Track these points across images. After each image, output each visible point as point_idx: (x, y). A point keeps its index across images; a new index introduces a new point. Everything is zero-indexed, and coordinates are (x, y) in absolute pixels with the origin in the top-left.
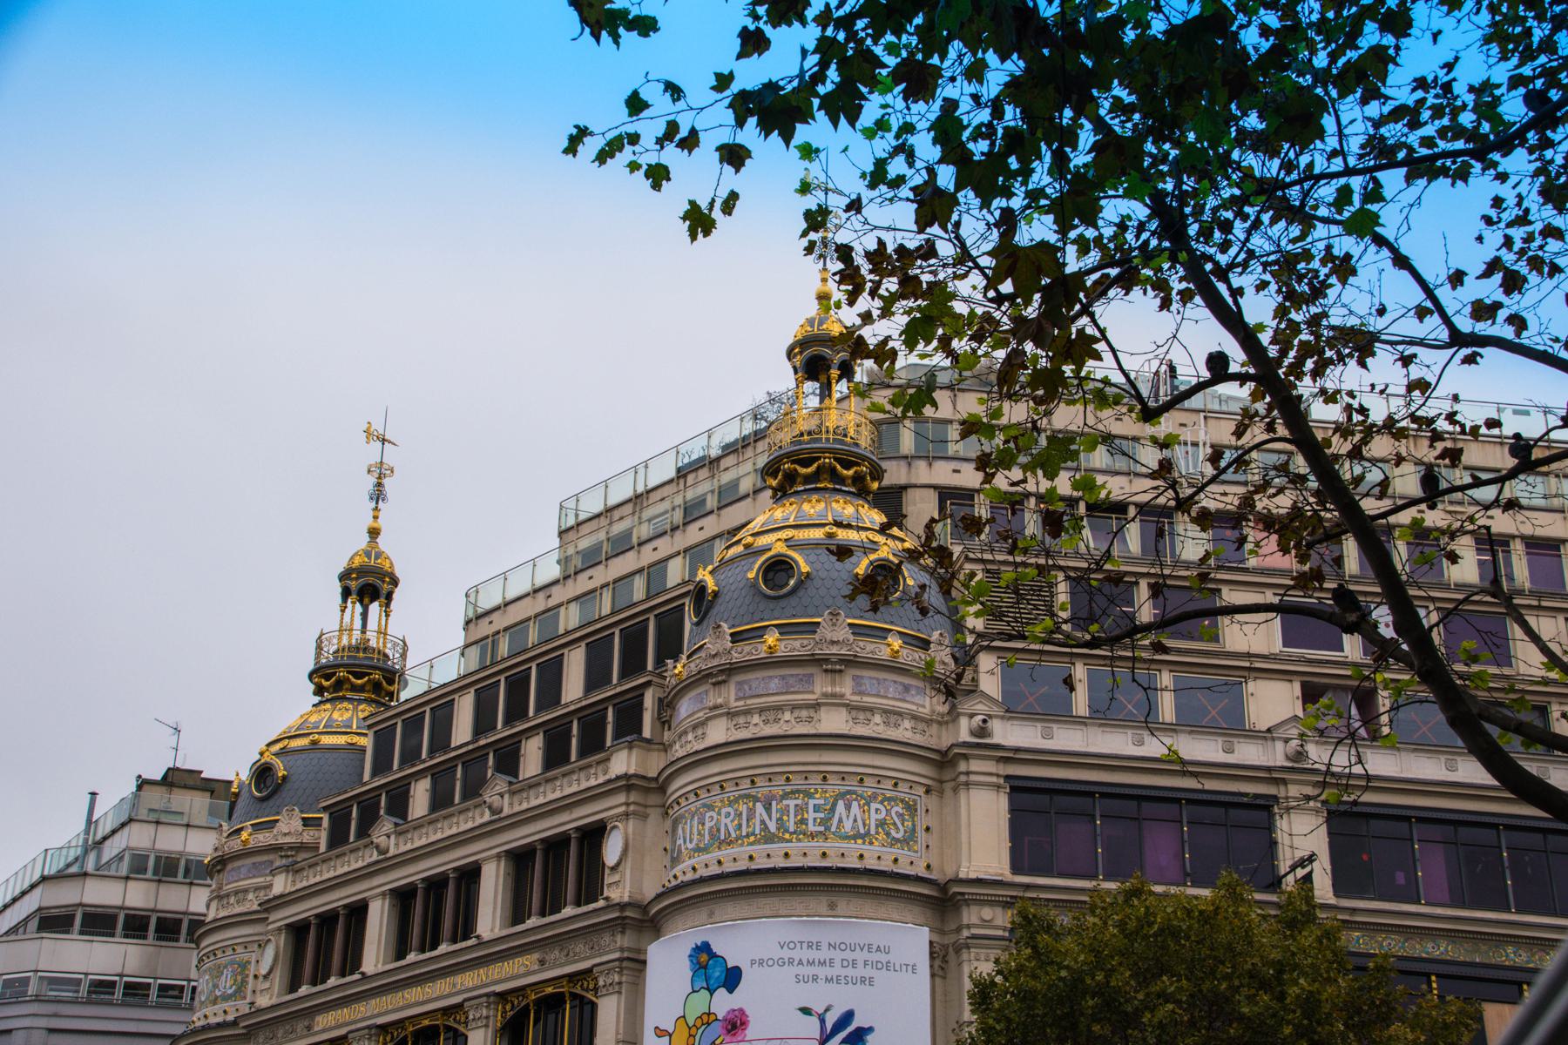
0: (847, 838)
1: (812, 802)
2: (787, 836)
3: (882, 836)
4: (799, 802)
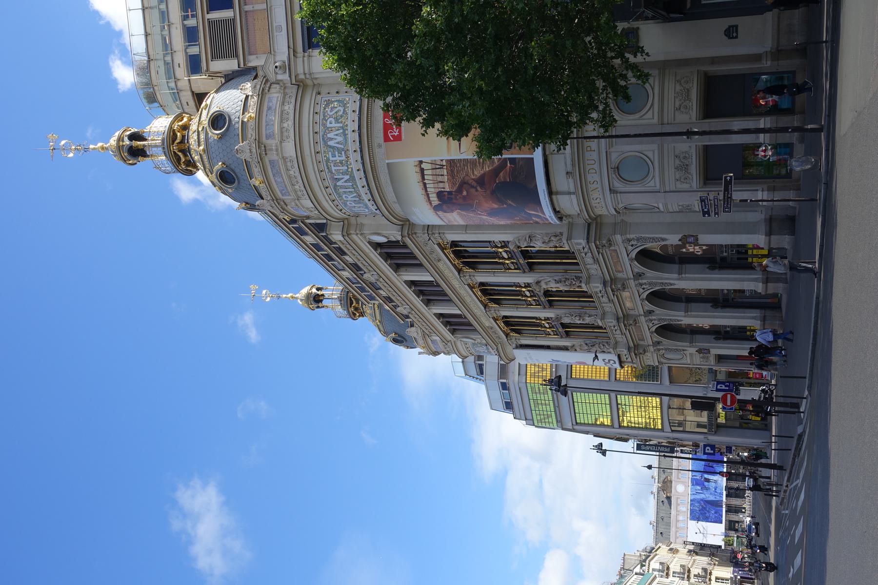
0: (346, 139)
1: (331, 158)
2: (350, 170)
3: (343, 120)
4: (332, 165)
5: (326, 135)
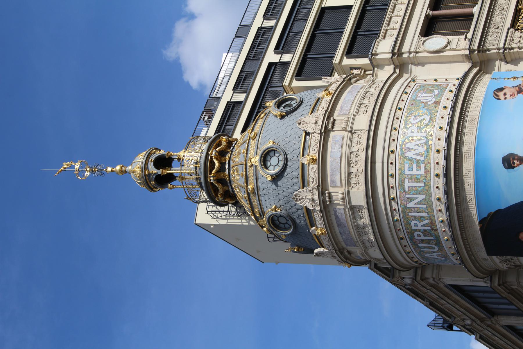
1: (407, 173)
3: (428, 129)
4: (406, 180)
5: (405, 145)
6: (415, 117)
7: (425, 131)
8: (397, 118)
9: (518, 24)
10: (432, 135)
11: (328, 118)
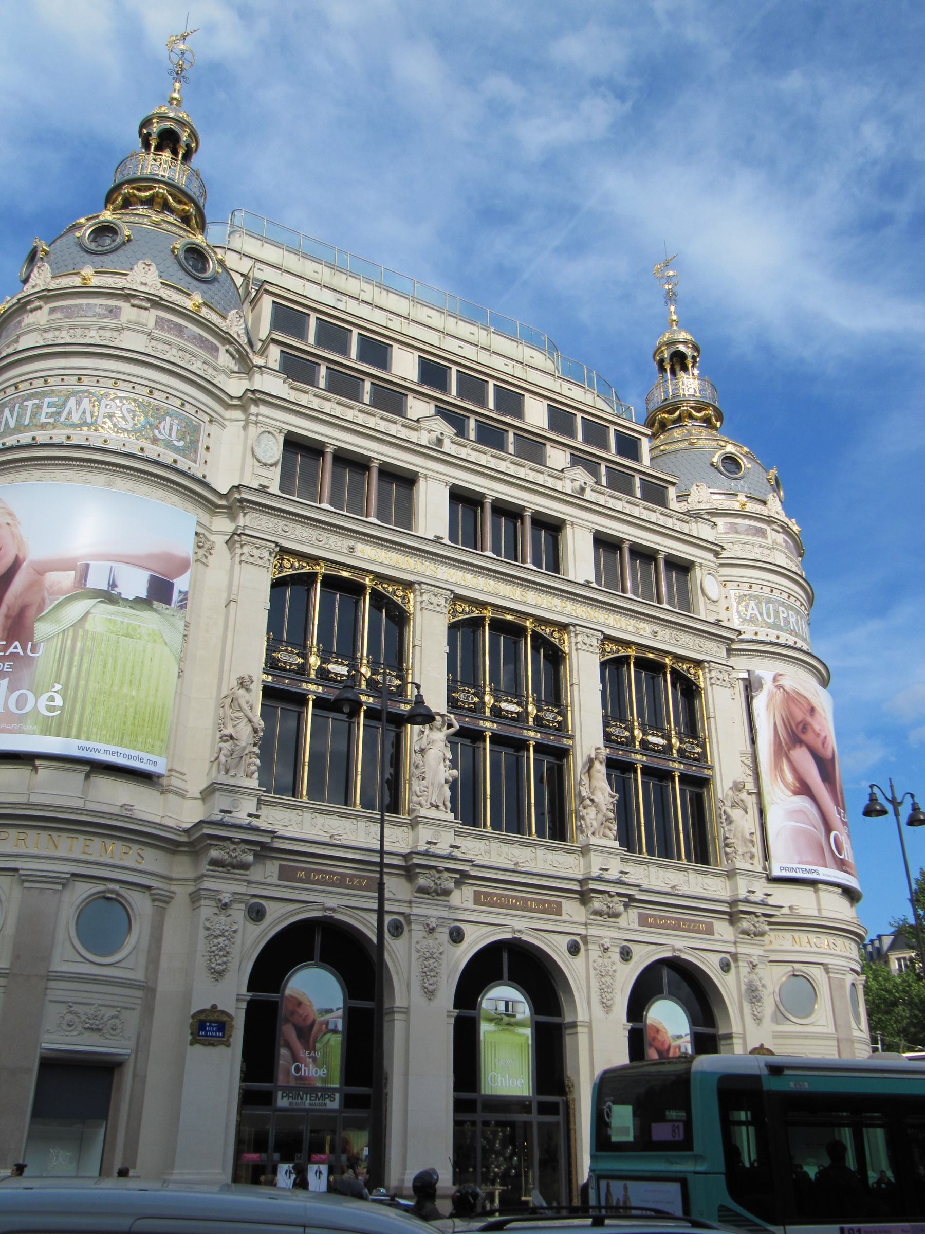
0: (74, 426)
6: (134, 411)
7: (105, 423)
8: (133, 387)
9: (292, 560)
10: (96, 430)
11: (149, 300)
